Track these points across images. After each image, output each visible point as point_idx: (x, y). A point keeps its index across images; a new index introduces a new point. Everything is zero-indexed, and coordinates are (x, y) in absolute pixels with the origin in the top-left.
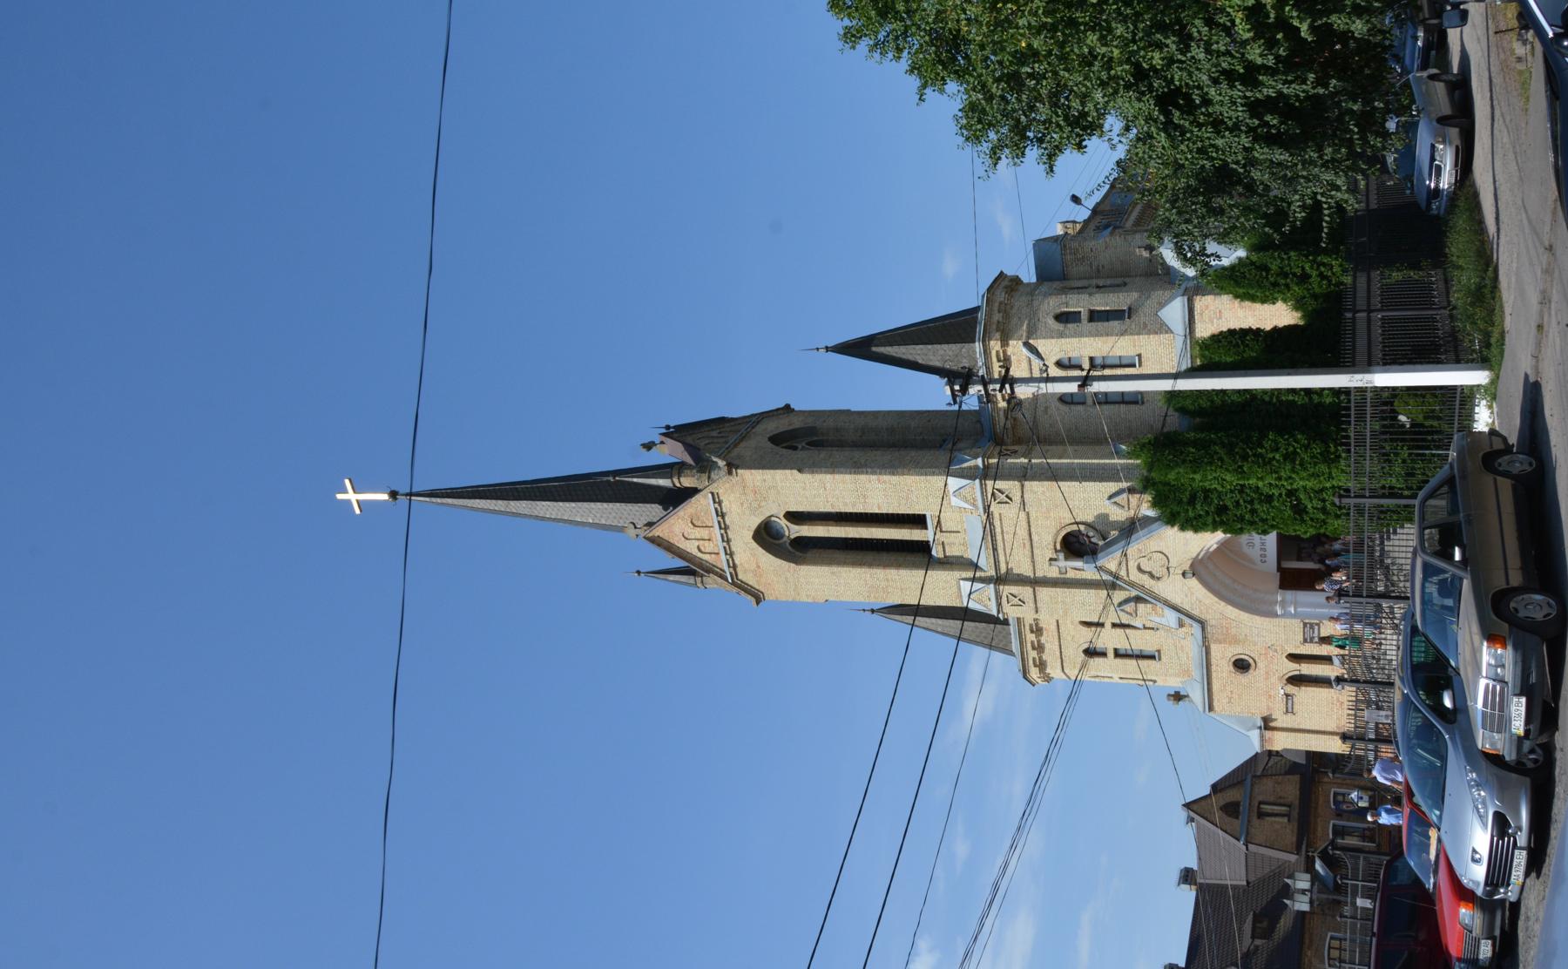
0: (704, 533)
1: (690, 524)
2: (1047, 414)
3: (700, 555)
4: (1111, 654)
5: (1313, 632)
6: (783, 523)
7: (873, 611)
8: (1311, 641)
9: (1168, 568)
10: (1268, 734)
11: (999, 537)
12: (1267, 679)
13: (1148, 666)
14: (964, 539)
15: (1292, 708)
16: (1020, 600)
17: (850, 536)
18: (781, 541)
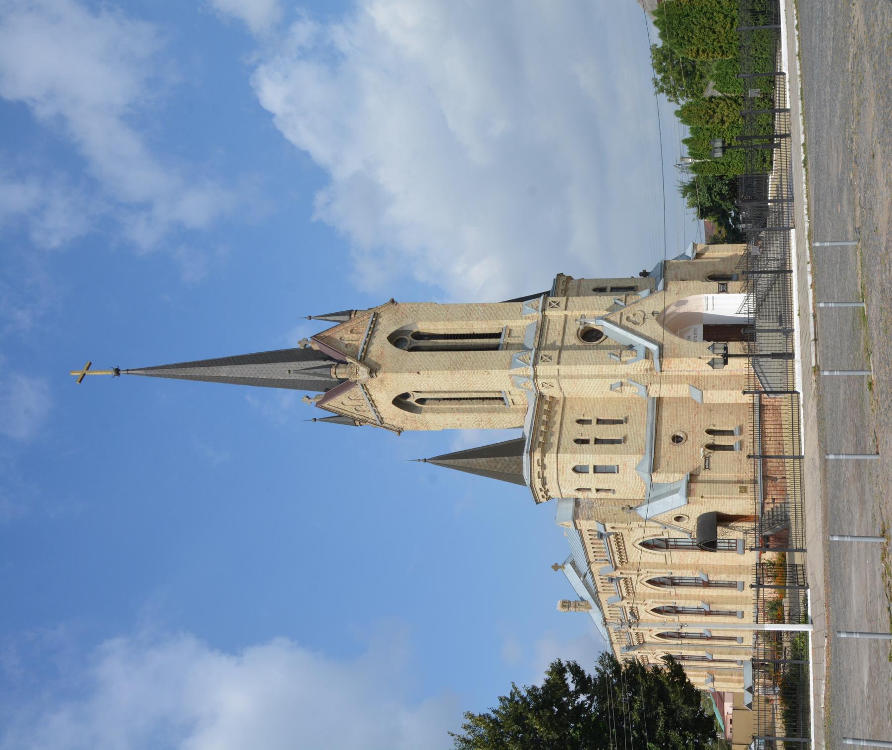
0: (354, 336)
1: (349, 332)
4: (592, 442)
6: (409, 338)
7: (425, 460)
9: (644, 319)
10: (693, 486)
12: (693, 446)
13: (616, 448)
15: (709, 466)
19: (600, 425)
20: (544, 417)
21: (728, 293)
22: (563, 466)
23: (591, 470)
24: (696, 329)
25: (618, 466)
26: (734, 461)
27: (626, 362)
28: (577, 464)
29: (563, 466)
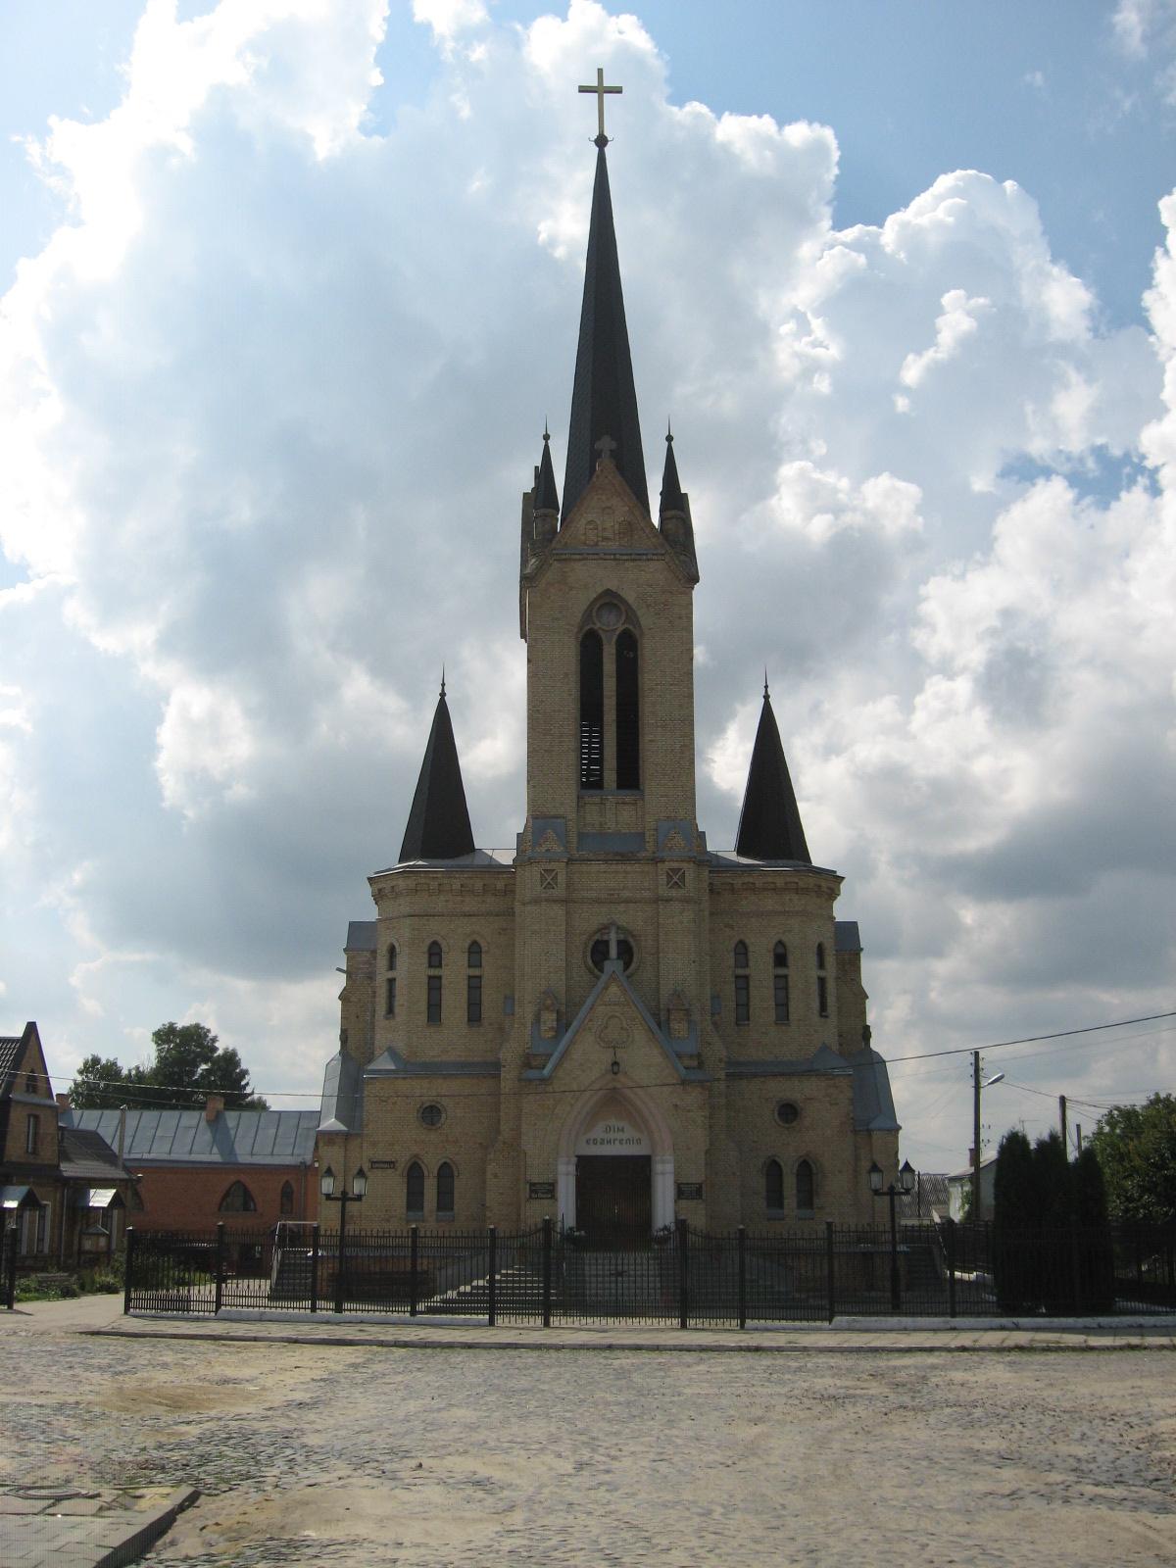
2: (725, 927)
3: (583, 521)
5: (543, 1193)
8: (531, 1191)
11: (620, 867)
14: (609, 828)
16: (549, 883)
17: (606, 701)
18: (595, 619)
19: (466, 982)
20: (478, 885)
21: (675, 1201)
22: (394, 927)
23: (390, 975)
24: (639, 1141)
25: (394, 1018)
26: (386, 1211)
27: (537, 1020)
28: (398, 950)
29: (394, 927)
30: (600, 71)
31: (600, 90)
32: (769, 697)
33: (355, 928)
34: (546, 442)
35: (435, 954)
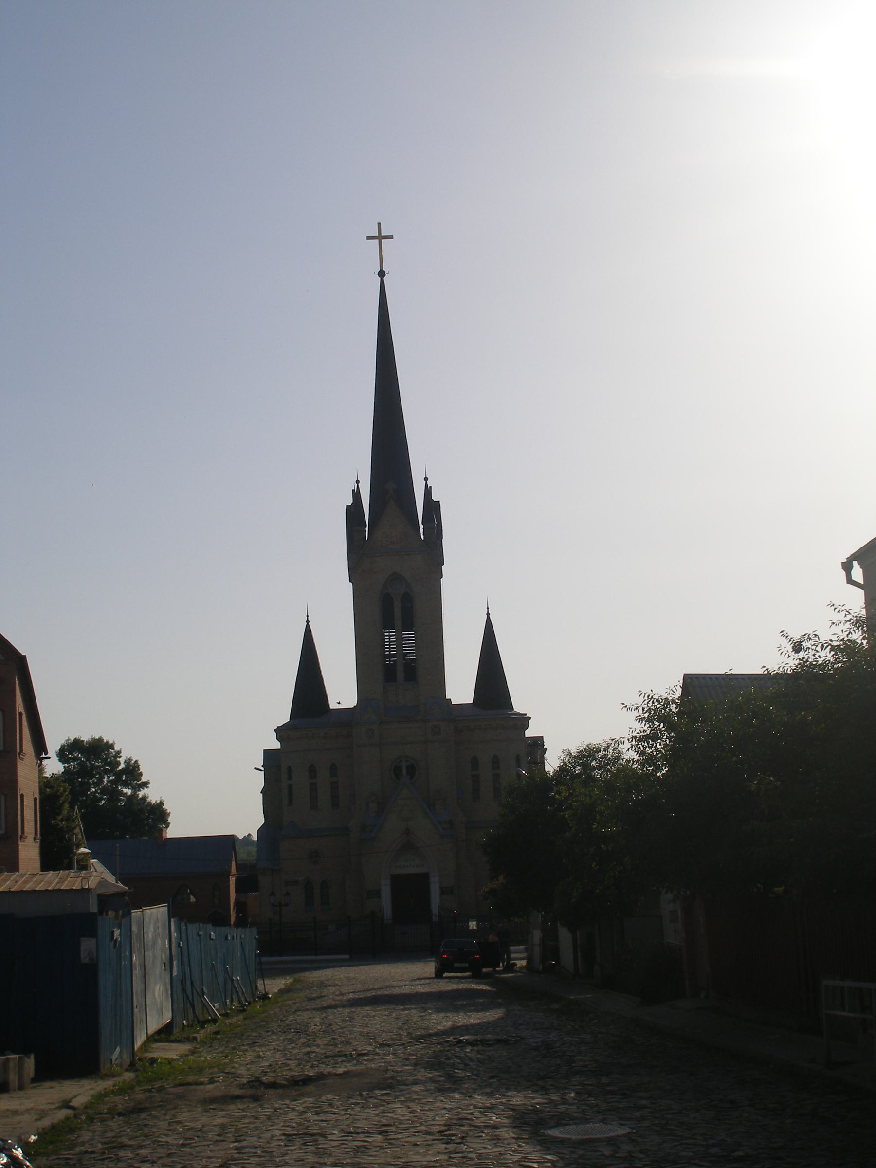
30: (379, 224)
31: (380, 238)
32: (489, 614)
33: (268, 754)
34: (358, 486)
35: (312, 771)
